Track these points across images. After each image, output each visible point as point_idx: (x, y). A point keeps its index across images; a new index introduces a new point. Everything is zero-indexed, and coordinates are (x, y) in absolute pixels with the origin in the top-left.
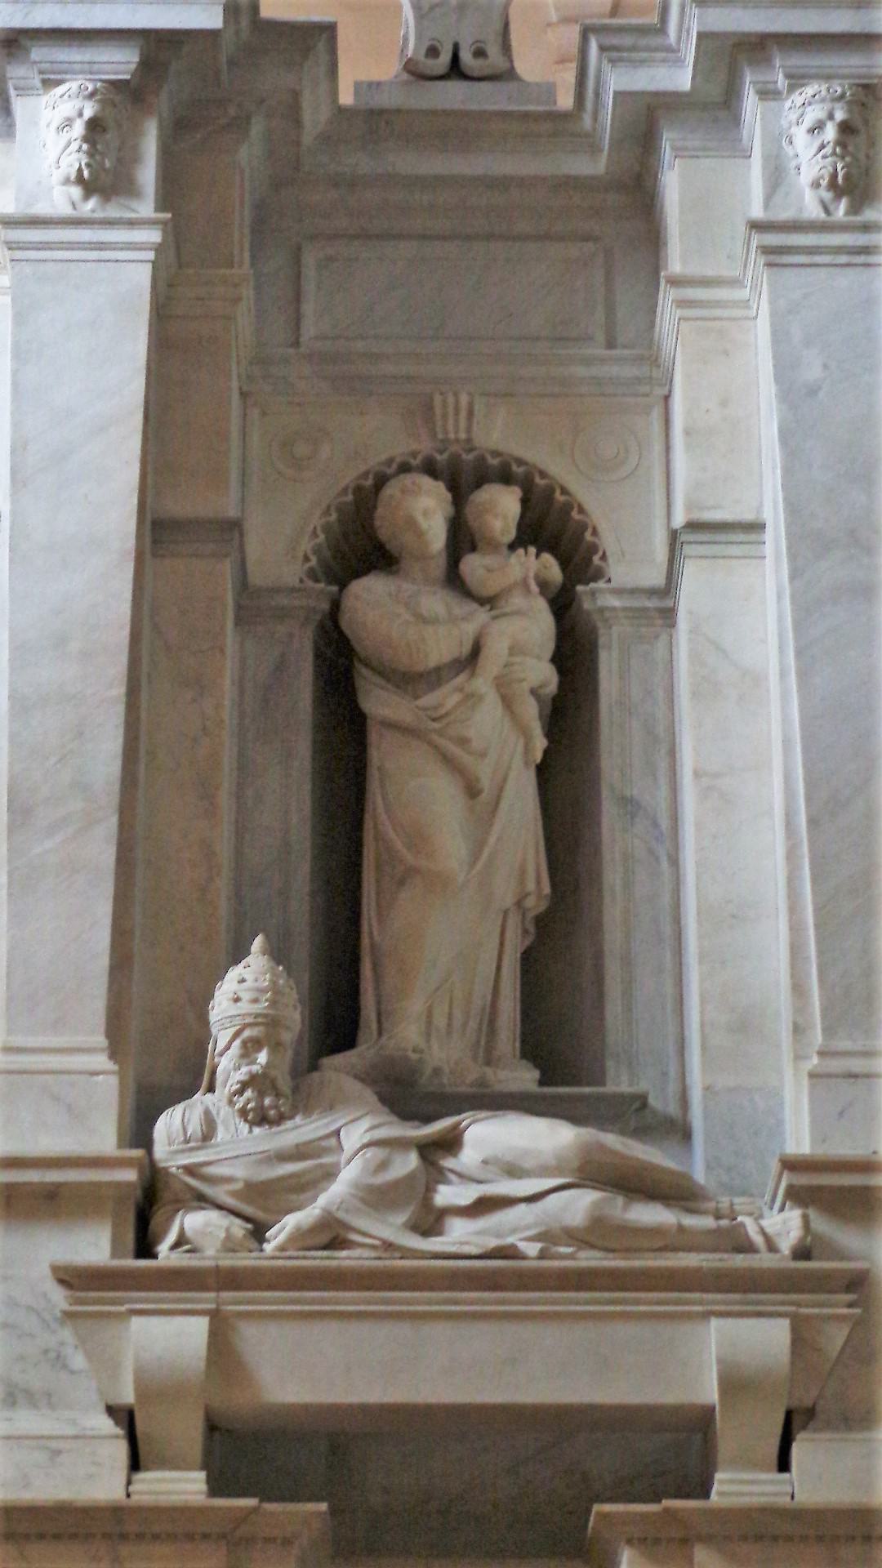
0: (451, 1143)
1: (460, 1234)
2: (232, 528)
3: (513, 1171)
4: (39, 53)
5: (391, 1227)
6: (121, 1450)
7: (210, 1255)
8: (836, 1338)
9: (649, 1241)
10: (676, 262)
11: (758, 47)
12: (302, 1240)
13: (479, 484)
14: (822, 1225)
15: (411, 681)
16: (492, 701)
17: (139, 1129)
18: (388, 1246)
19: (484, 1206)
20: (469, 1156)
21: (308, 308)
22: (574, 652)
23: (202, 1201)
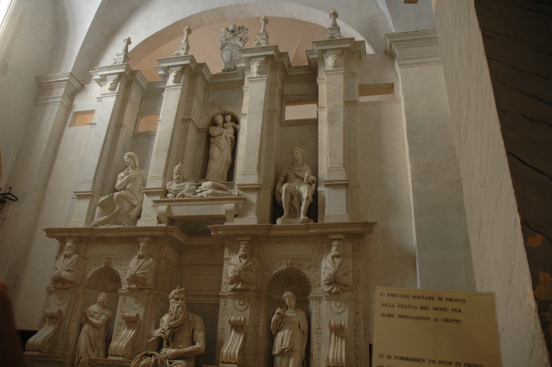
0: (200, 185)
1: (199, 195)
5: (190, 195)
6: (156, 221)
7: (170, 199)
8: (241, 206)
10: (245, 86)
11: (250, 59)
13: (226, 115)
14: (241, 192)
15: (214, 137)
18: (189, 197)
20: (202, 187)
21: (210, 98)
22: (236, 133)
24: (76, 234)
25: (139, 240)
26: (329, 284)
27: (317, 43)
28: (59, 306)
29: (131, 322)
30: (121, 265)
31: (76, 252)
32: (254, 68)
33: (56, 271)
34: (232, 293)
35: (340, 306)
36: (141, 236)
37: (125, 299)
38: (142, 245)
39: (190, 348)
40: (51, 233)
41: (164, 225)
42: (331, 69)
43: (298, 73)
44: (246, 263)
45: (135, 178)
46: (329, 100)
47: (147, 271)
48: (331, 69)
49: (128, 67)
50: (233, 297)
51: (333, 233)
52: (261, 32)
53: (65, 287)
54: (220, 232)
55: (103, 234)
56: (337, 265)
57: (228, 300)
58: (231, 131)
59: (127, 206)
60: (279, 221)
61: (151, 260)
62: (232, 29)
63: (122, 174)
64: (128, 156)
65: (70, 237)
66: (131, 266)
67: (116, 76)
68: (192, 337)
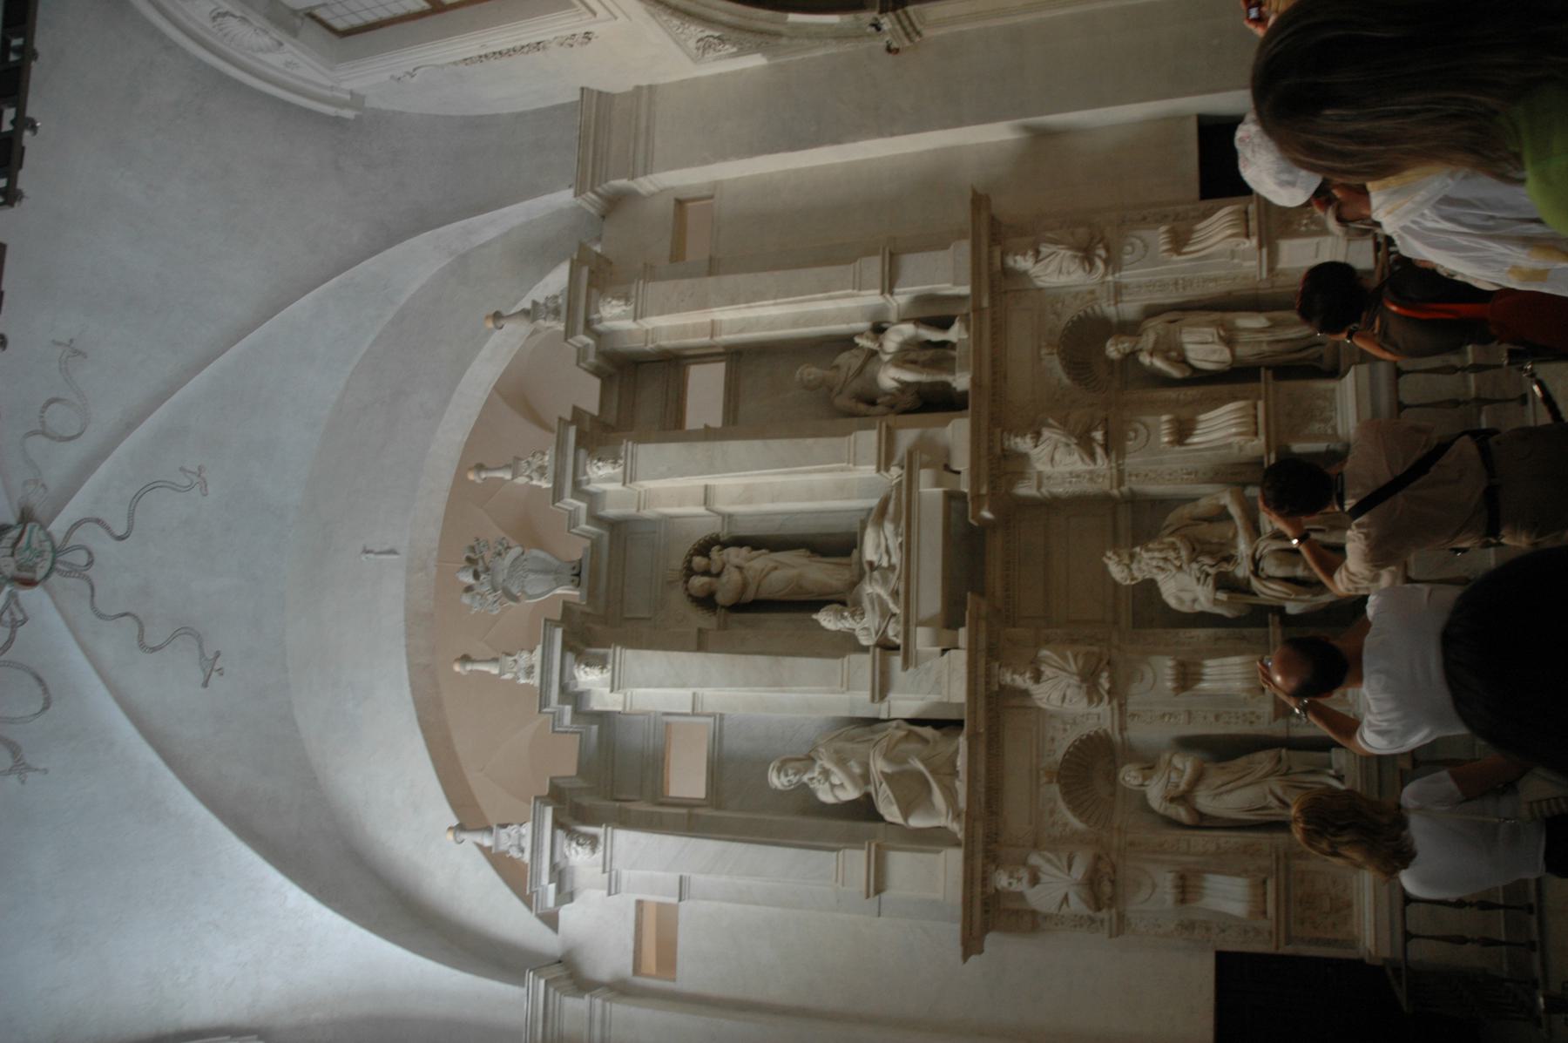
0: (871, 564)
1: (895, 560)
2: (700, 631)
3: (878, 546)
4: (566, 680)
5: (893, 578)
7: (900, 628)
8: (926, 458)
9: (897, 508)
10: (631, 511)
11: (576, 484)
12: (896, 602)
15: (745, 586)
16: (752, 563)
17: (865, 649)
19: (888, 552)
22: (739, 542)
23: (885, 631)
24: (979, 862)
25: (996, 688)
26: (1092, 264)
27: (569, 332)
28: (1154, 886)
29: (1187, 677)
30: (1053, 739)
31: (1024, 864)
32: (601, 475)
33: (1073, 898)
34: (1113, 456)
35: (1132, 244)
36: (987, 683)
37: (1133, 715)
38: (1008, 678)
39: (1234, 510)
40: (971, 944)
41: (963, 634)
42: (630, 308)
43: (615, 405)
44: (1050, 426)
45: (837, 752)
46: (703, 305)
47: (1069, 654)
48: (630, 308)
49: (543, 800)
50: (1122, 454)
51: (991, 264)
52: (507, 476)
53: (1109, 869)
54: (984, 491)
55: (981, 787)
56: (1052, 248)
57: (1128, 469)
58: (732, 551)
59: (913, 746)
60: (961, 381)
61: (1045, 653)
62: (471, 571)
63: (826, 796)
64: (779, 771)
65: (985, 880)
66: (1059, 695)
67: (560, 833)
68: (1209, 520)
